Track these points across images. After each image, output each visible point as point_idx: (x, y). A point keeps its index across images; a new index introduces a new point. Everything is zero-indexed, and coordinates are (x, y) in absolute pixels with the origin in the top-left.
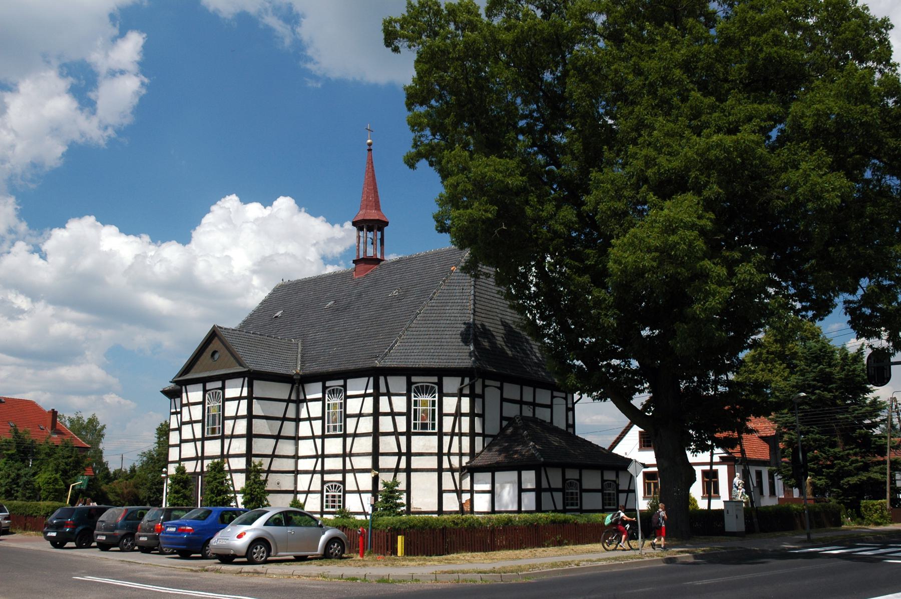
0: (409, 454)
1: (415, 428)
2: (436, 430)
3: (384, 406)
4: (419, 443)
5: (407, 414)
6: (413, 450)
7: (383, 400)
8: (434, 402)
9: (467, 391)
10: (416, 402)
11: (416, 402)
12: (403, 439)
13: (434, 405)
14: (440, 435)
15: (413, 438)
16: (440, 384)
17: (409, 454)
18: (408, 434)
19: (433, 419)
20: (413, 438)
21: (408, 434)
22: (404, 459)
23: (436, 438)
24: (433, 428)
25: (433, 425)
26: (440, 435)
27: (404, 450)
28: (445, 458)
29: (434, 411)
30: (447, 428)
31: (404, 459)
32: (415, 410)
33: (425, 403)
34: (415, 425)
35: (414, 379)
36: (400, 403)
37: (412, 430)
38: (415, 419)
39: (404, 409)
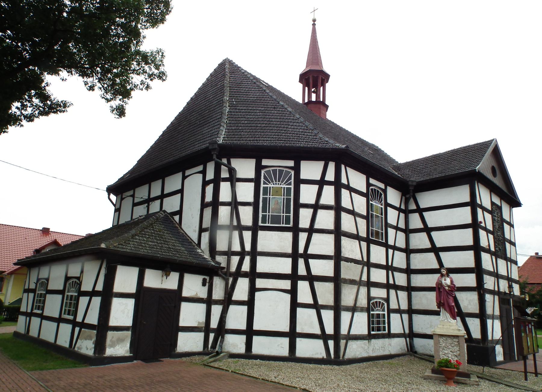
0: (254, 254)
1: (264, 221)
2: (291, 225)
3: (225, 194)
4: (269, 240)
5: (255, 205)
6: (259, 249)
7: (225, 188)
8: (289, 190)
9: (330, 176)
10: (265, 189)
11: (265, 189)
12: (247, 235)
13: (289, 193)
14: (296, 230)
15: (261, 233)
16: (297, 169)
17: (254, 254)
18: (255, 229)
19: (288, 211)
20: (261, 233)
21: (255, 229)
22: (247, 259)
23: (289, 235)
24: (288, 222)
25: (288, 218)
26: (296, 230)
27: (248, 248)
28: (301, 262)
29: (288, 200)
30: (304, 221)
31: (247, 259)
32: (265, 200)
33: (277, 192)
34: (264, 217)
35: (265, 162)
36: (245, 192)
37: (260, 224)
38: (264, 210)
39: (250, 199)
